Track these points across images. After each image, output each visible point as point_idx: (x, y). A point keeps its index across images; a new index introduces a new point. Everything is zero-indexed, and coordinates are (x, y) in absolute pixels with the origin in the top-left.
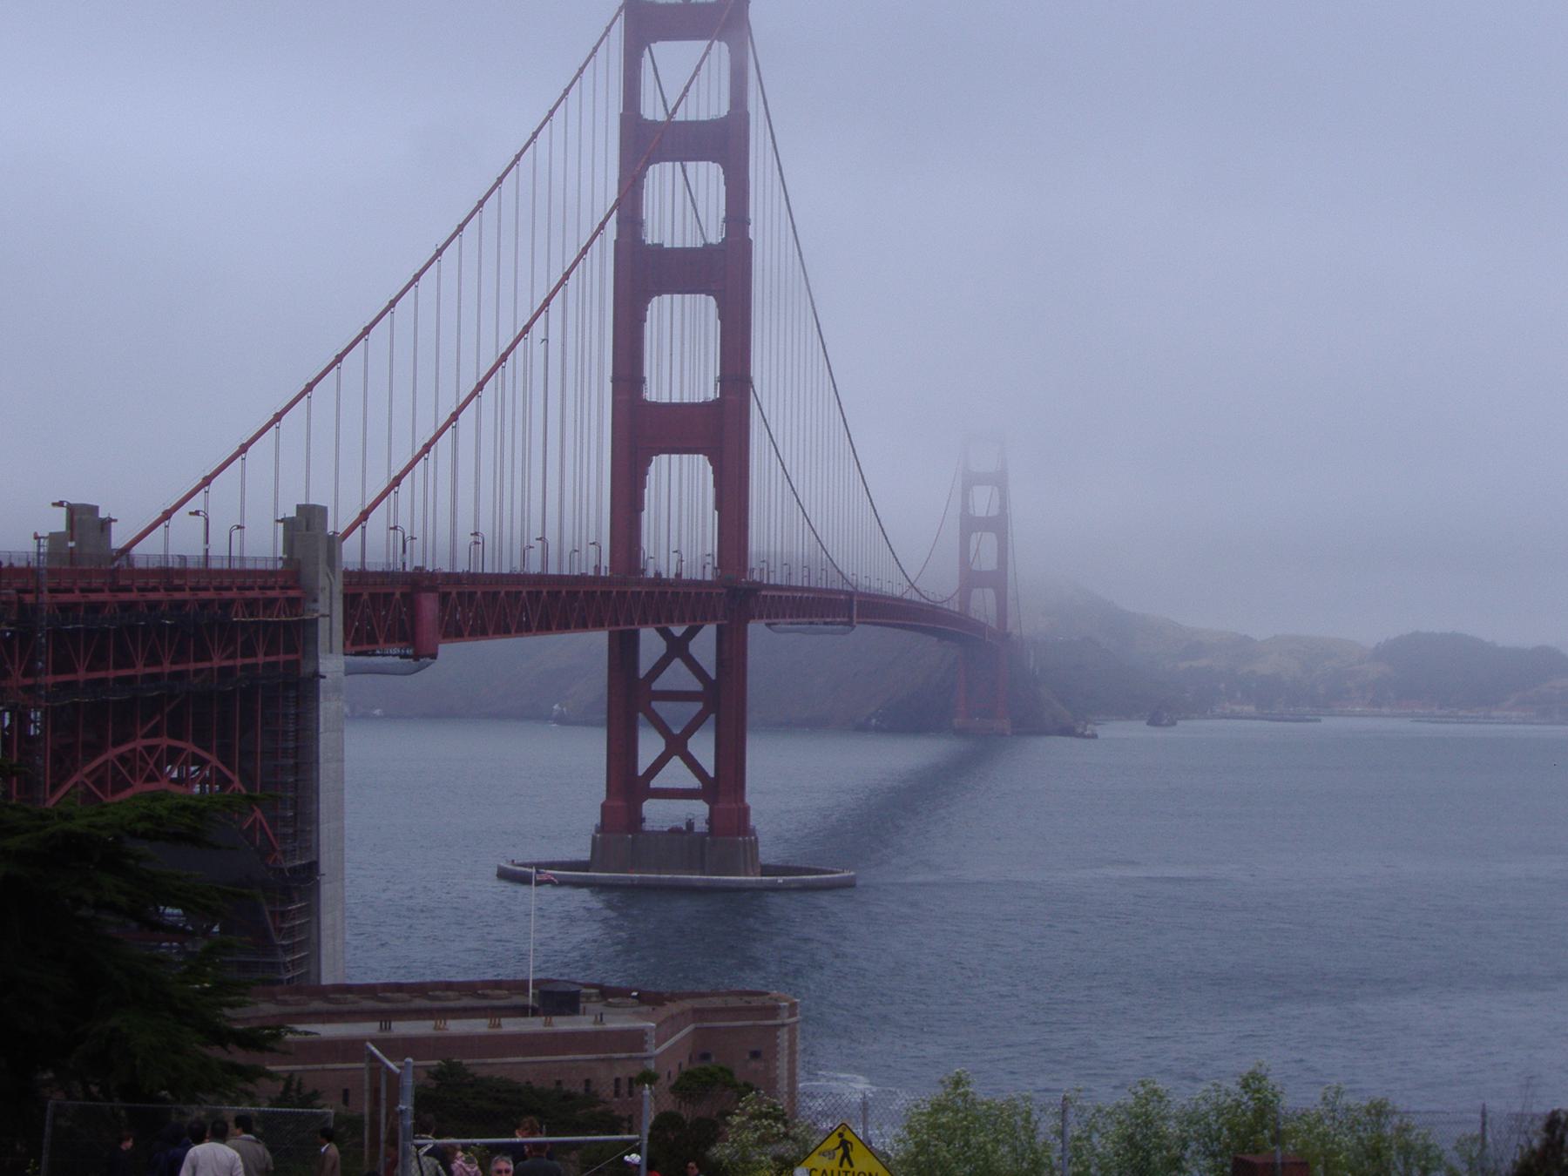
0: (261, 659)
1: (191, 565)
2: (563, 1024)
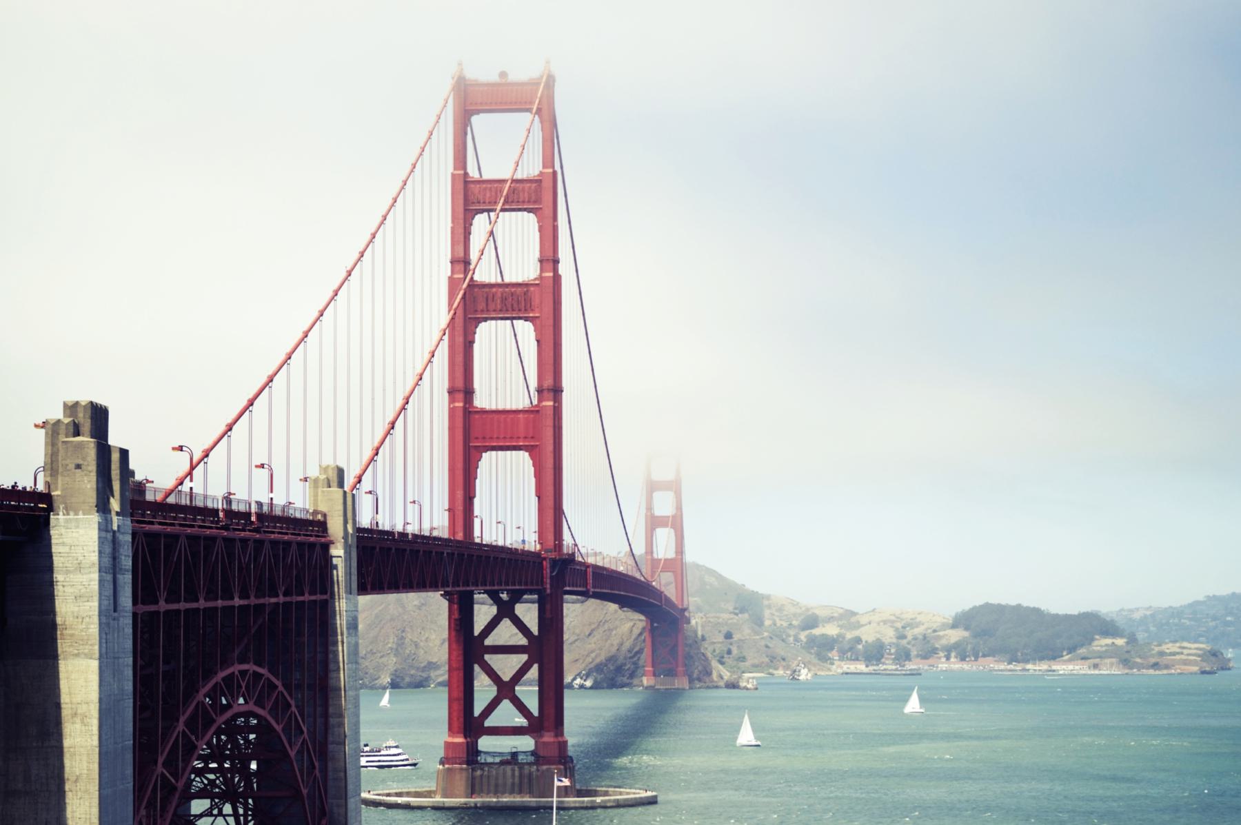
0: (307, 597)
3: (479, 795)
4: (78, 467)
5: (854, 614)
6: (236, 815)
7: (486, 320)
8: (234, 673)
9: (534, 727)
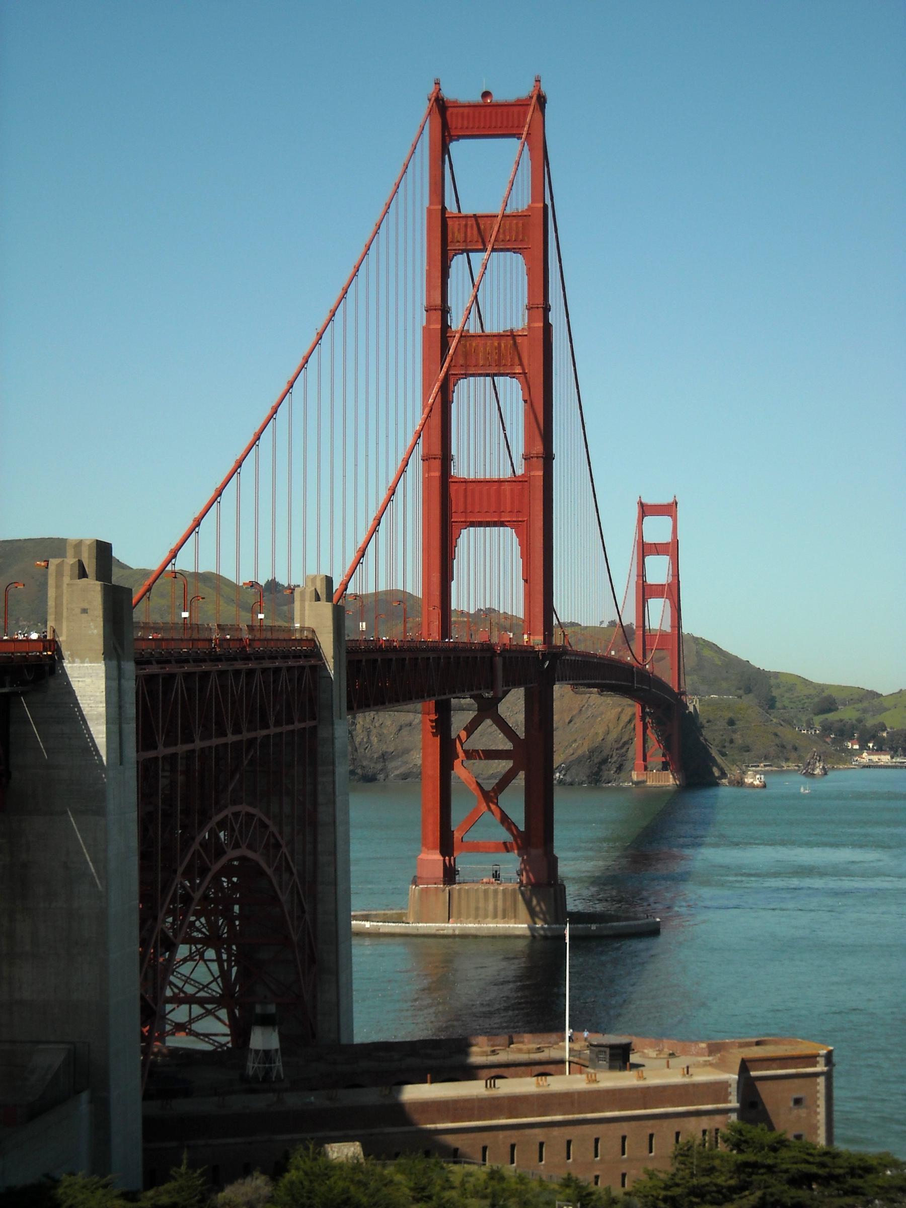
0: (298, 726)
3: (459, 919)
4: (84, 611)
5: (879, 696)
6: (219, 960)
7: (466, 376)
8: (227, 816)
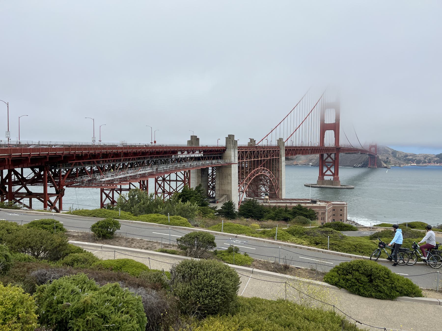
0: (274, 158)
1: (266, 146)
2: (314, 205)
9: (333, 175)
